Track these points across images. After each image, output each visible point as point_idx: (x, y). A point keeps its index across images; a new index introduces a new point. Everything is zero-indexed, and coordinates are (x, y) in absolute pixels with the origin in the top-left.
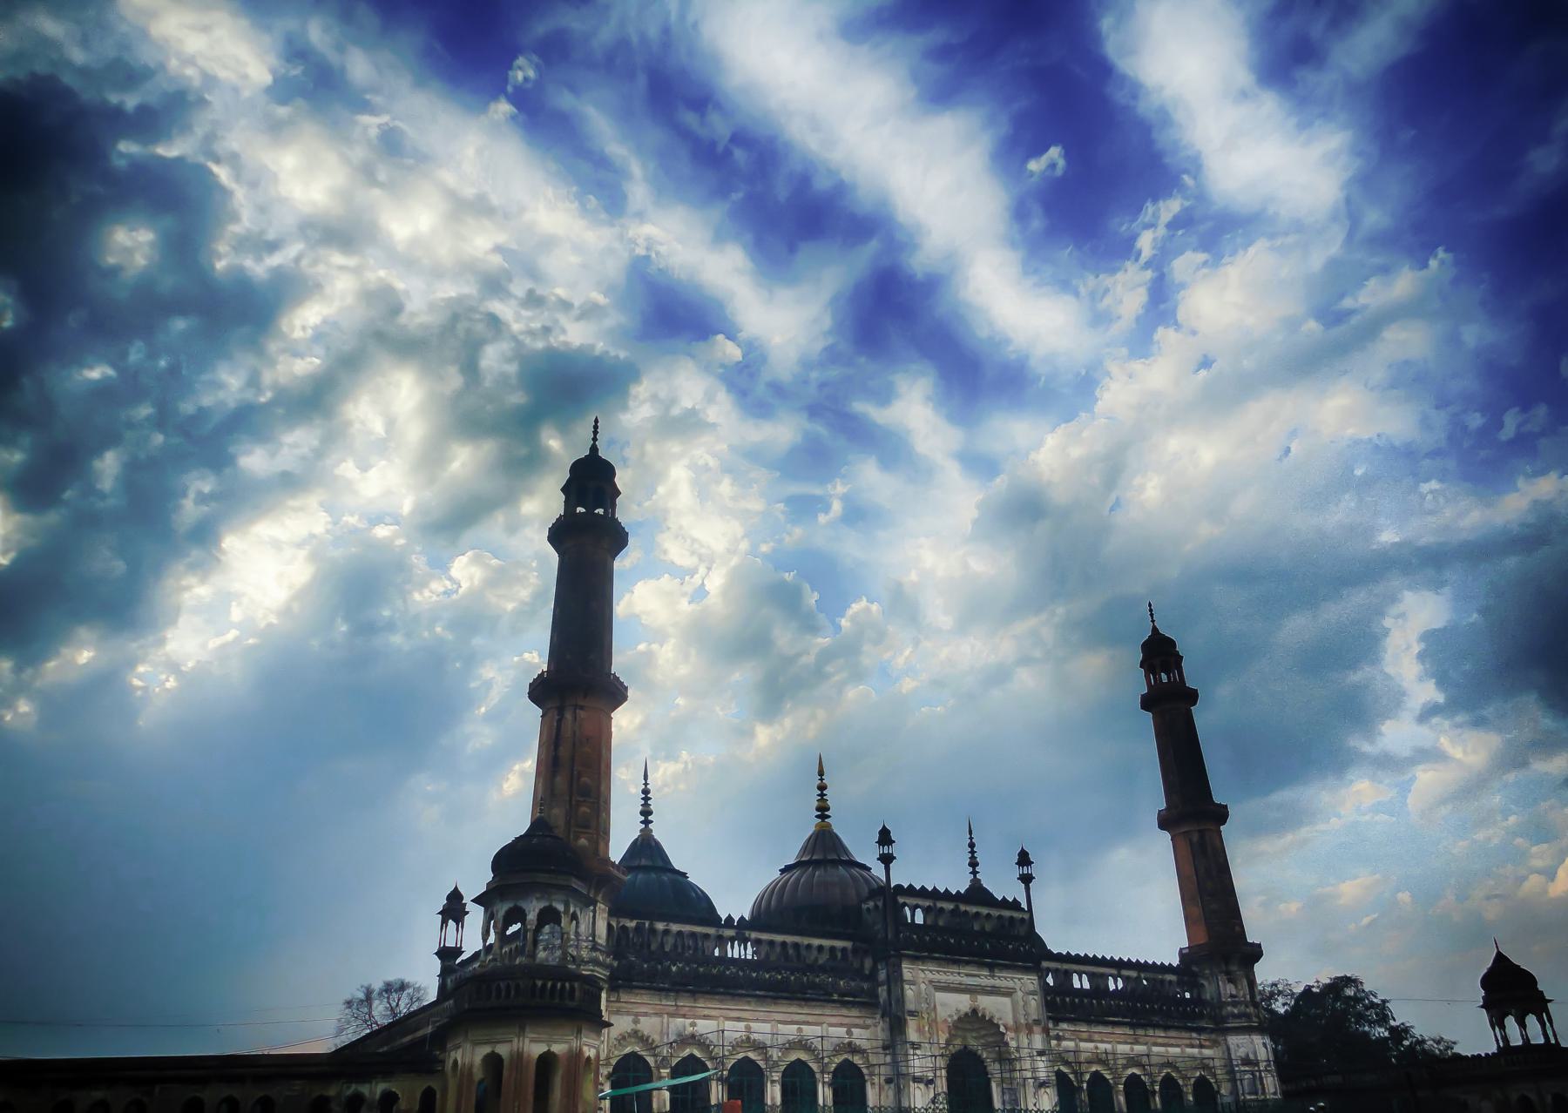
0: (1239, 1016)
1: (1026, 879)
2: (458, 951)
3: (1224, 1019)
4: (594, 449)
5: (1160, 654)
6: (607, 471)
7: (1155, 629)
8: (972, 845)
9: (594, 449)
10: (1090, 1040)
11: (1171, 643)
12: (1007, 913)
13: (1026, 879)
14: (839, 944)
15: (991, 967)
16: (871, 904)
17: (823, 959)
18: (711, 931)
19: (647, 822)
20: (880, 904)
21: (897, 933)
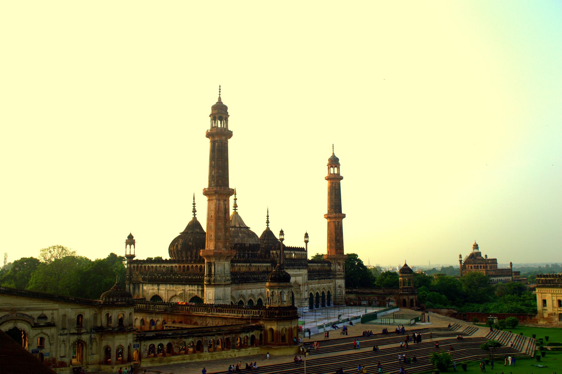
0: (340, 275)
1: (306, 242)
2: (134, 256)
3: (336, 275)
4: (220, 99)
5: (334, 162)
6: (225, 108)
7: (333, 154)
8: (268, 216)
9: (220, 99)
10: (311, 284)
11: (337, 160)
12: (303, 253)
13: (306, 242)
14: (268, 264)
15: (299, 269)
16: (274, 252)
17: (265, 269)
18: (245, 264)
19: (195, 215)
20: (279, 253)
21: (284, 261)
